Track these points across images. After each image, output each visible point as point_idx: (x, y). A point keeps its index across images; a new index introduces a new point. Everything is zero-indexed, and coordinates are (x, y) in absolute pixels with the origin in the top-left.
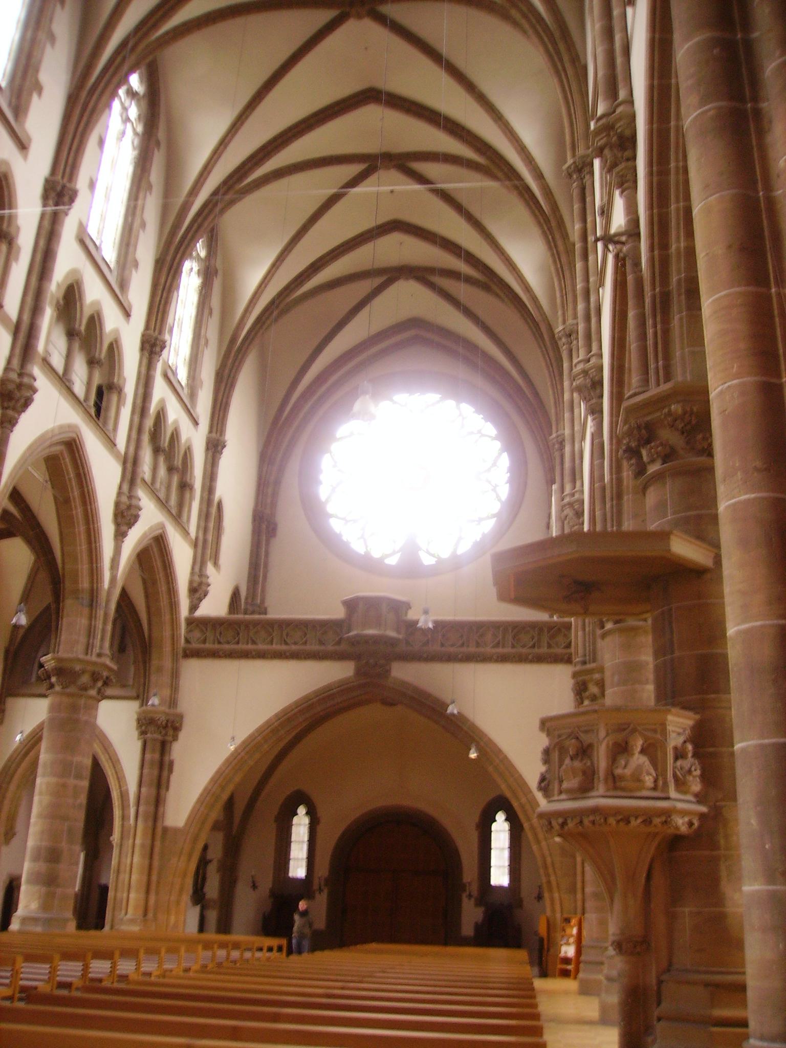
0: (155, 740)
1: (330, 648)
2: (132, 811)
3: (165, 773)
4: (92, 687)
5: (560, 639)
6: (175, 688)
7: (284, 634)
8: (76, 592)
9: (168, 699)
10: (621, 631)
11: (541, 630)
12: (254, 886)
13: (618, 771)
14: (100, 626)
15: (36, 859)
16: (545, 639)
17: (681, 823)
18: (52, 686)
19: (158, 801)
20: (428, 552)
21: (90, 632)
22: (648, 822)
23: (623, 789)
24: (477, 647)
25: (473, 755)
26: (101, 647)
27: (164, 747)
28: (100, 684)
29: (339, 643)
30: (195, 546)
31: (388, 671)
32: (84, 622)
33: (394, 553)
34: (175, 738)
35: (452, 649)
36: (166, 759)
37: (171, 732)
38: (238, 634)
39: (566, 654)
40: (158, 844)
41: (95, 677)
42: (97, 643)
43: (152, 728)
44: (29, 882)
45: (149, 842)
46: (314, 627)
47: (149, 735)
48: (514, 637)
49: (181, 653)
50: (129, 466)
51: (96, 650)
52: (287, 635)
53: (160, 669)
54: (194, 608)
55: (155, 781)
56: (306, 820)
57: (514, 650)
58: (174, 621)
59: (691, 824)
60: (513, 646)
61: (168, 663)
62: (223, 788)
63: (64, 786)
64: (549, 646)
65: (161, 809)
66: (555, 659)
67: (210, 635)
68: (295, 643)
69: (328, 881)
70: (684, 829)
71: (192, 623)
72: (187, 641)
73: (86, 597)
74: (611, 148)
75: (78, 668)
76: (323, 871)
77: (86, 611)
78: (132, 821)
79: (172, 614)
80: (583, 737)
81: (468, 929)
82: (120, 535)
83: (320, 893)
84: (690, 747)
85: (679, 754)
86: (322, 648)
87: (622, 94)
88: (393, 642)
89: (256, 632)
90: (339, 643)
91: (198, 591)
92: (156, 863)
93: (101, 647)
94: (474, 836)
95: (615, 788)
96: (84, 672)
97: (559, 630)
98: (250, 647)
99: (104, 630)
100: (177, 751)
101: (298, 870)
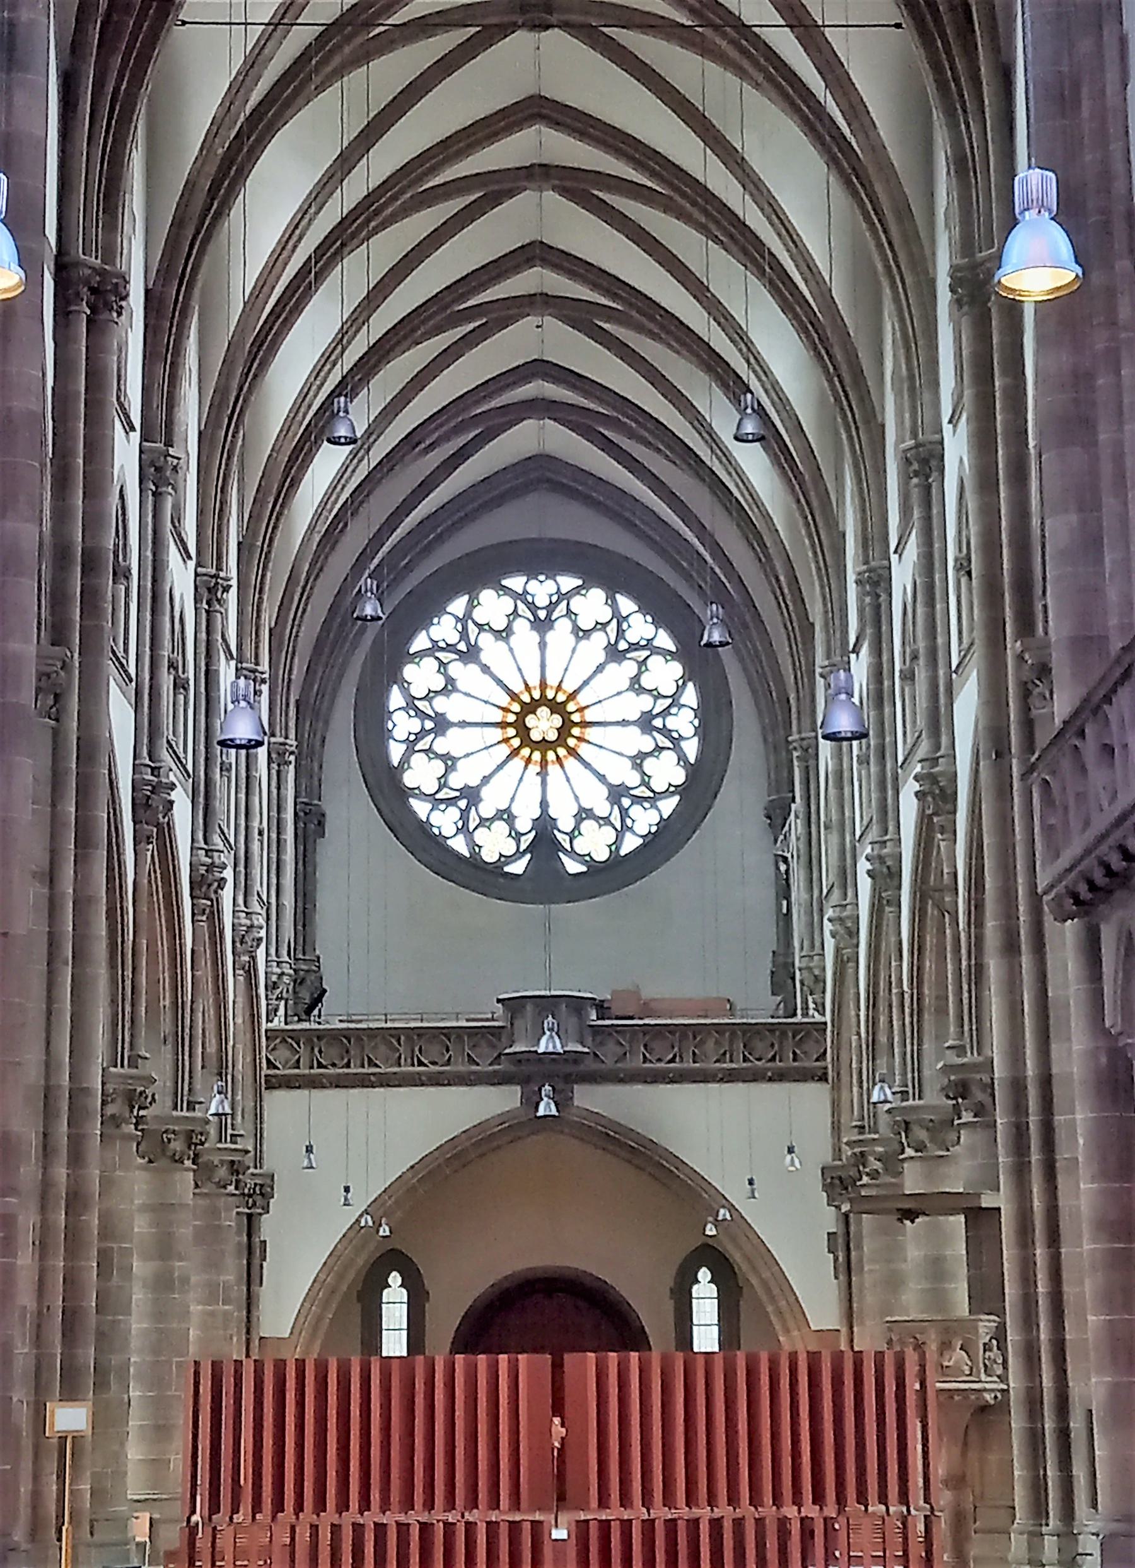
1: (484, 1068)
3: (256, 1261)
11: (784, 1034)
13: (946, 1364)
17: (988, 1397)
22: (966, 1398)
23: (948, 1376)
24: (694, 1062)
27: (251, 1223)
29: (497, 1060)
33: (518, 854)
38: (347, 1052)
51: (230, 1131)
59: (996, 1397)
60: (745, 1059)
62: (341, 1277)
65: (254, 1313)
68: (434, 1063)
70: (992, 1402)
71: (271, 1035)
74: (934, 799)
80: (918, 1336)
84: (994, 1342)
85: (987, 1348)
86: (474, 1068)
87: (944, 740)
88: (575, 1058)
94: (669, 1306)
95: (944, 1375)
96: (222, 1162)
97: (808, 1034)
100: (268, 1227)
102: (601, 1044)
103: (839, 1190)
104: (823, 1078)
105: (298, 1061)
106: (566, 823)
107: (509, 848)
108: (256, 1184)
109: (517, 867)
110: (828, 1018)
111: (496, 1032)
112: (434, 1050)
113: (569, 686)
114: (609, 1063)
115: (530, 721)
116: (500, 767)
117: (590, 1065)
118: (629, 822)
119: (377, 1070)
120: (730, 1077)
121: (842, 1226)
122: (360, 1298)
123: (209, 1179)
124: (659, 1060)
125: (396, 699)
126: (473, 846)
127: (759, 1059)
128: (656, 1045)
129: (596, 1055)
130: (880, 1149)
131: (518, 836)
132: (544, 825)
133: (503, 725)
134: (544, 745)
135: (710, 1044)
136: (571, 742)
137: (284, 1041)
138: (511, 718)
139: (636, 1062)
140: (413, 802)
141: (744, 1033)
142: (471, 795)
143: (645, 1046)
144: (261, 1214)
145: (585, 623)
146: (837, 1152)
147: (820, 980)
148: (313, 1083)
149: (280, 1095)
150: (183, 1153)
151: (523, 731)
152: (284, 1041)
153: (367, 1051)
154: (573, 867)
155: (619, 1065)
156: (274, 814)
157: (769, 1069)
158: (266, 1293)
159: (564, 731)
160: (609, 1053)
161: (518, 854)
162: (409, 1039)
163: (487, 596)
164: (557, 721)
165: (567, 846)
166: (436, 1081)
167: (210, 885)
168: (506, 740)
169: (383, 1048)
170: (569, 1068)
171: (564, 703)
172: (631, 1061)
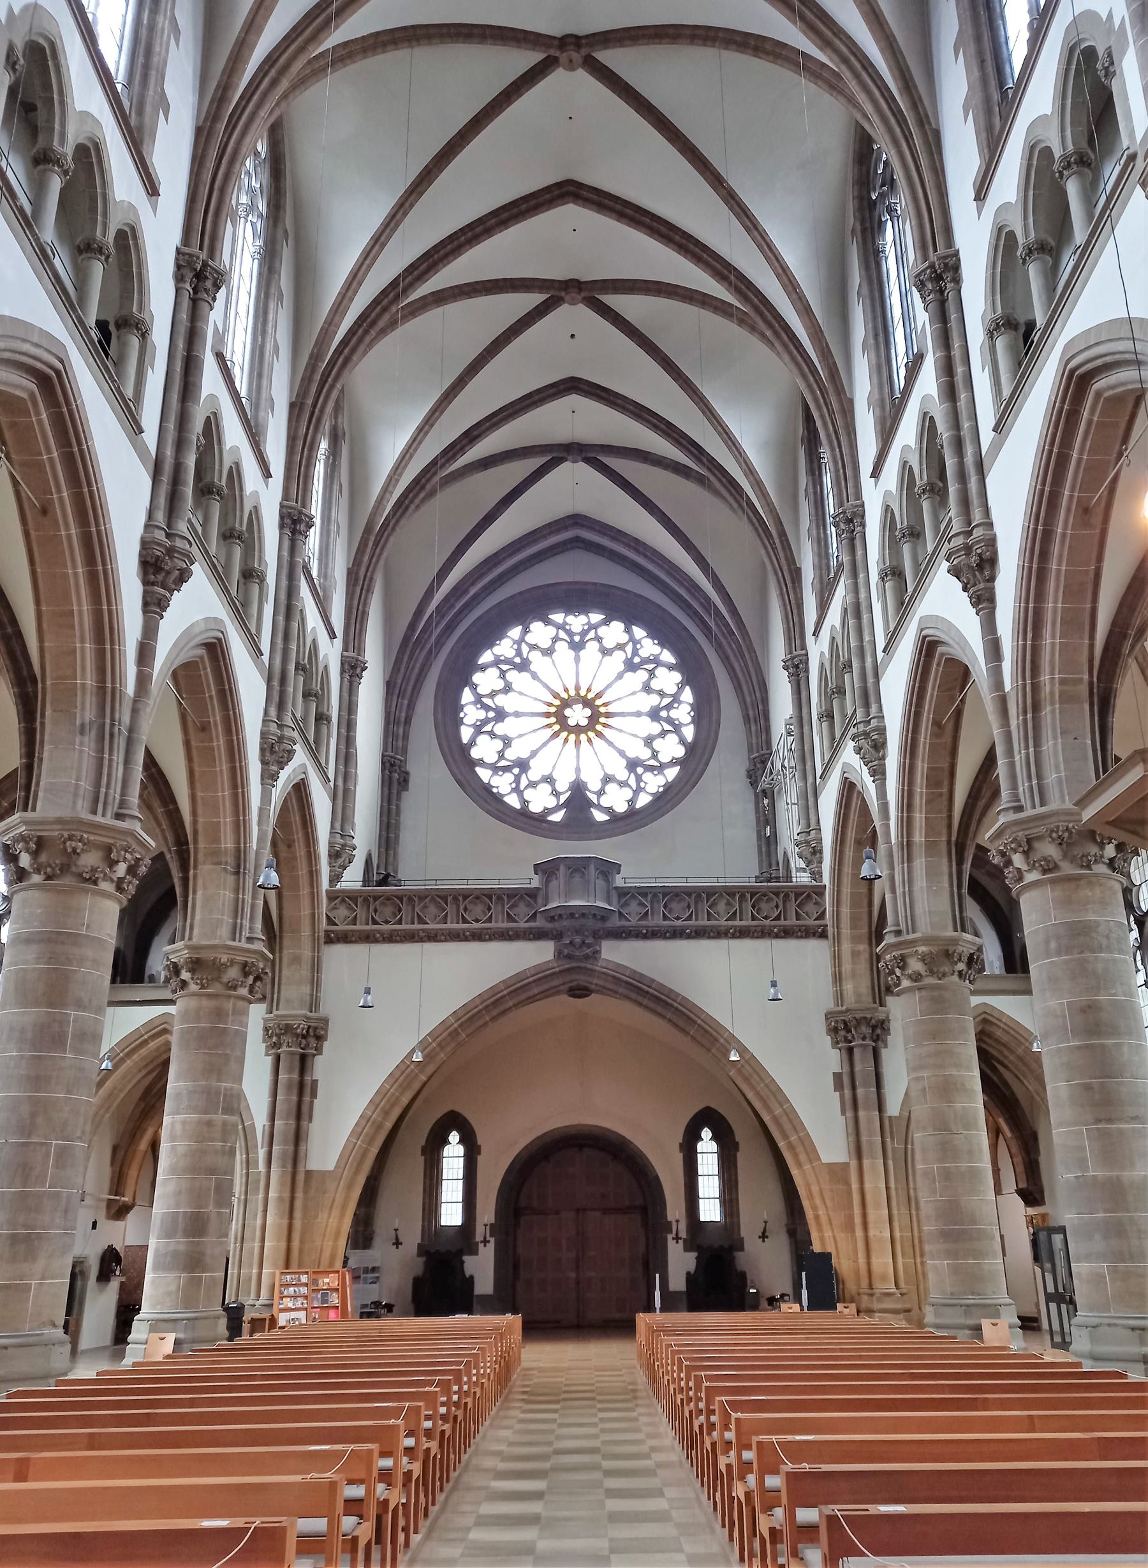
0: (292, 1053)
1: (522, 925)
2: (262, 1153)
3: (307, 1099)
4: (243, 985)
5: (810, 907)
6: (315, 983)
7: (462, 908)
8: (215, 855)
9: (308, 998)
10: (1053, 882)
11: (787, 896)
12: (397, 1243)
14: (248, 898)
15: (169, 1232)
16: (792, 907)
18: (184, 984)
19: (298, 1137)
20: (599, 807)
21: (237, 909)
25: (734, 1057)
26: (251, 929)
27: (304, 1063)
28: (251, 979)
29: (533, 917)
30: (334, 798)
31: (599, 952)
32: (229, 895)
34: (319, 1050)
35: (678, 923)
36: (308, 1078)
37: (313, 1042)
38: (400, 910)
39: (820, 926)
40: (299, 1195)
41: (245, 969)
42: (246, 923)
43: (286, 1039)
44: (156, 1268)
45: (287, 1195)
46: (499, 898)
47: (284, 1048)
48: (753, 906)
49: (322, 940)
50: (276, 683)
51: (246, 933)
52: (465, 909)
53: (296, 960)
54: (335, 878)
55: (294, 1109)
56: (460, 1150)
57: (754, 923)
58: (314, 896)
60: (754, 918)
61: (307, 953)
62: (386, 1113)
63: (209, 1124)
64: (798, 917)
65: (302, 1148)
66: (807, 933)
67: (361, 912)
68: (477, 921)
69: (494, 1229)
72: (330, 921)
73: (231, 860)
75: (224, 959)
76: (486, 1214)
77: (231, 879)
78: (262, 1167)
79: (312, 886)
81: (678, 1283)
82: (269, 778)
83: (485, 1246)
88: (603, 916)
89: (425, 907)
90: (533, 917)
91: (340, 855)
92: (298, 1223)
93: (251, 929)
94: (678, 1158)
96: (232, 962)
97: (809, 896)
98: (417, 926)
99: (253, 906)
100: (321, 1067)
101: (451, 1215)
102: (626, 904)
103: (842, 1033)
104: (823, 935)
105: (355, 917)
106: (594, 784)
107: (551, 802)
108: (309, 1027)
109: (557, 817)
110: (826, 880)
111: (532, 894)
112: (478, 909)
113: (596, 689)
114: (633, 921)
115: (568, 712)
116: (545, 744)
117: (615, 922)
118: (642, 785)
119: (426, 926)
120: (742, 933)
121: (846, 1069)
122: (424, 1151)
123: (218, 979)
124: (678, 918)
125: (467, 696)
126: (525, 802)
127: (766, 918)
128: (674, 905)
129: (620, 914)
130: (922, 949)
131: (556, 794)
132: (578, 788)
133: (547, 715)
134: (578, 729)
135: (721, 907)
136: (599, 727)
137: (343, 901)
138: (553, 710)
139: (656, 921)
140: (478, 770)
141: (753, 895)
142: (523, 765)
143: (665, 906)
144: (314, 1055)
145: (609, 644)
146: (839, 997)
147: (817, 852)
148: (368, 938)
149: (340, 949)
150: (94, 870)
151: (562, 719)
152: (343, 901)
153: (417, 909)
154: (600, 817)
155: (644, 923)
156: (345, 714)
157: (775, 927)
158: (315, 1130)
159: (594, 719)
160: (634, 908)
161: (558, 808)
162: (455, 899)
163: (537, 627)
164: (588, 712)
165: (593, 798)
166: (477, 936)
167: (168, 573)
168: (549, 726)
169: (432, 909)
170: (599, 925)
171: (594, 699)
172: (652, 919)
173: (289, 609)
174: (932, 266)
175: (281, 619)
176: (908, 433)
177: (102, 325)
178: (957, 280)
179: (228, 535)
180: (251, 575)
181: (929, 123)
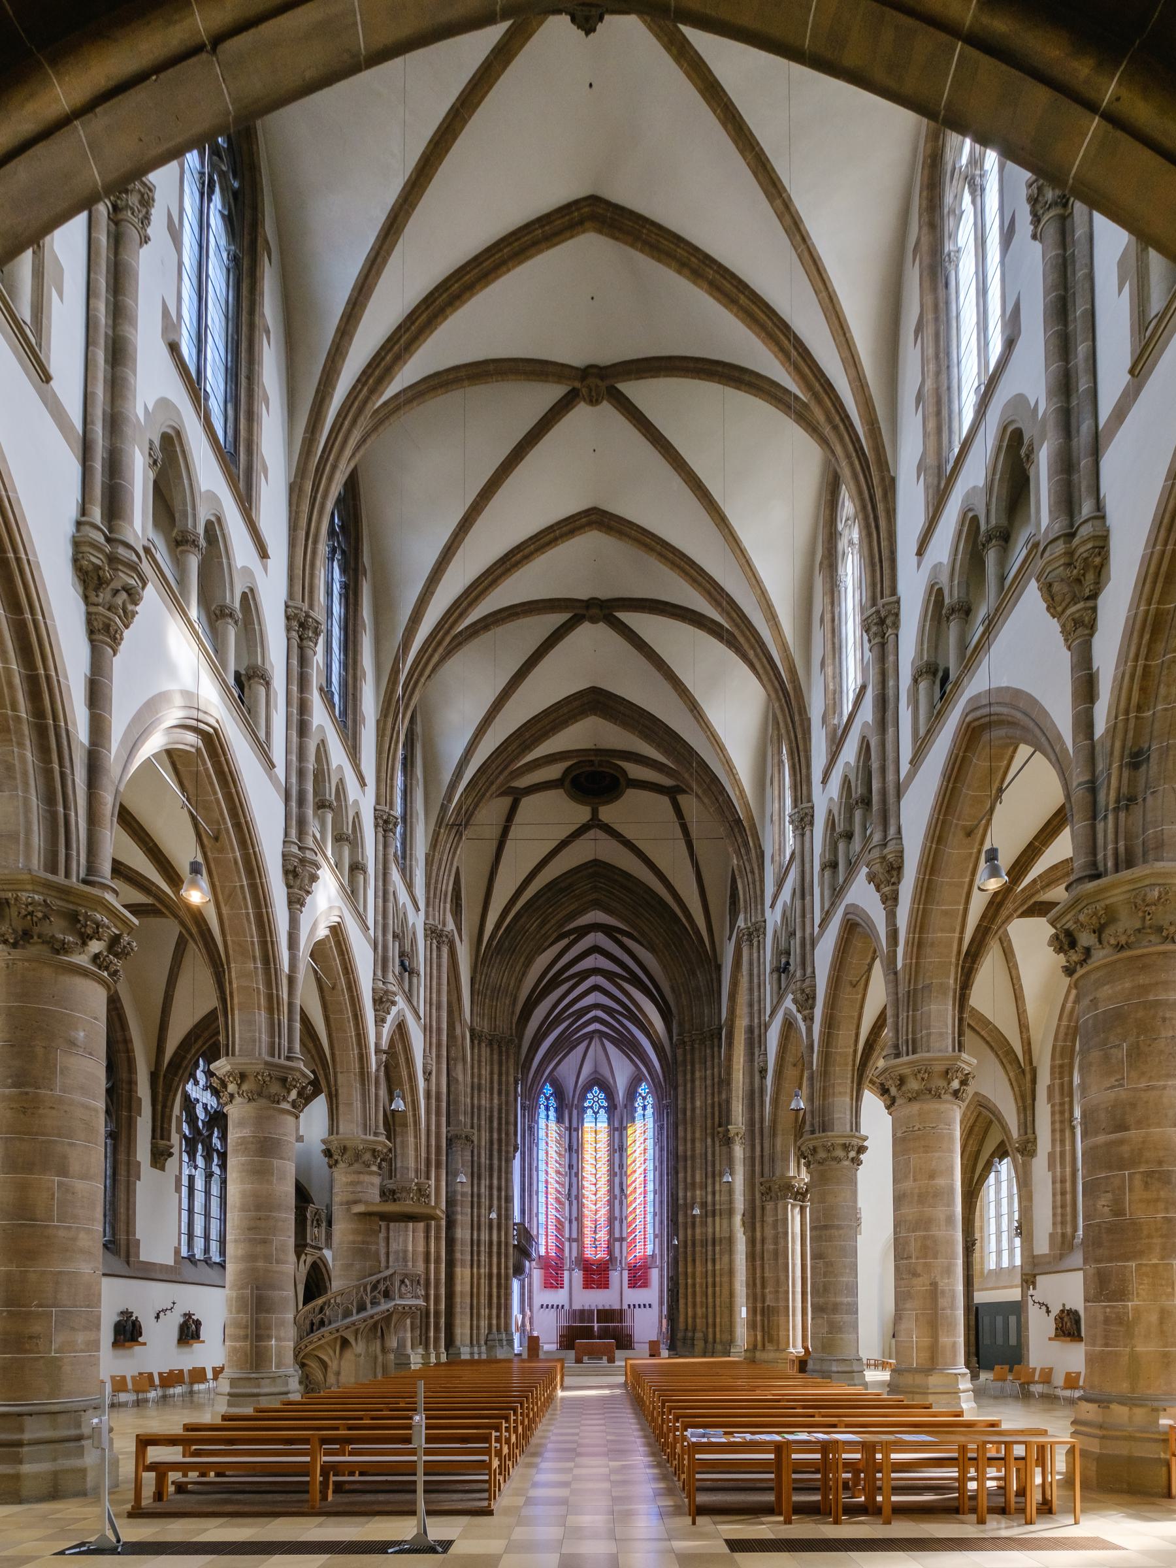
173: (385, 894)
174: (878, 612)
175: (380, 901)
176: (849, 753)
177: (238, 676)
178: (896, 625)
179: (339, 839)
180: (356, 868)
181: (889, 471)
